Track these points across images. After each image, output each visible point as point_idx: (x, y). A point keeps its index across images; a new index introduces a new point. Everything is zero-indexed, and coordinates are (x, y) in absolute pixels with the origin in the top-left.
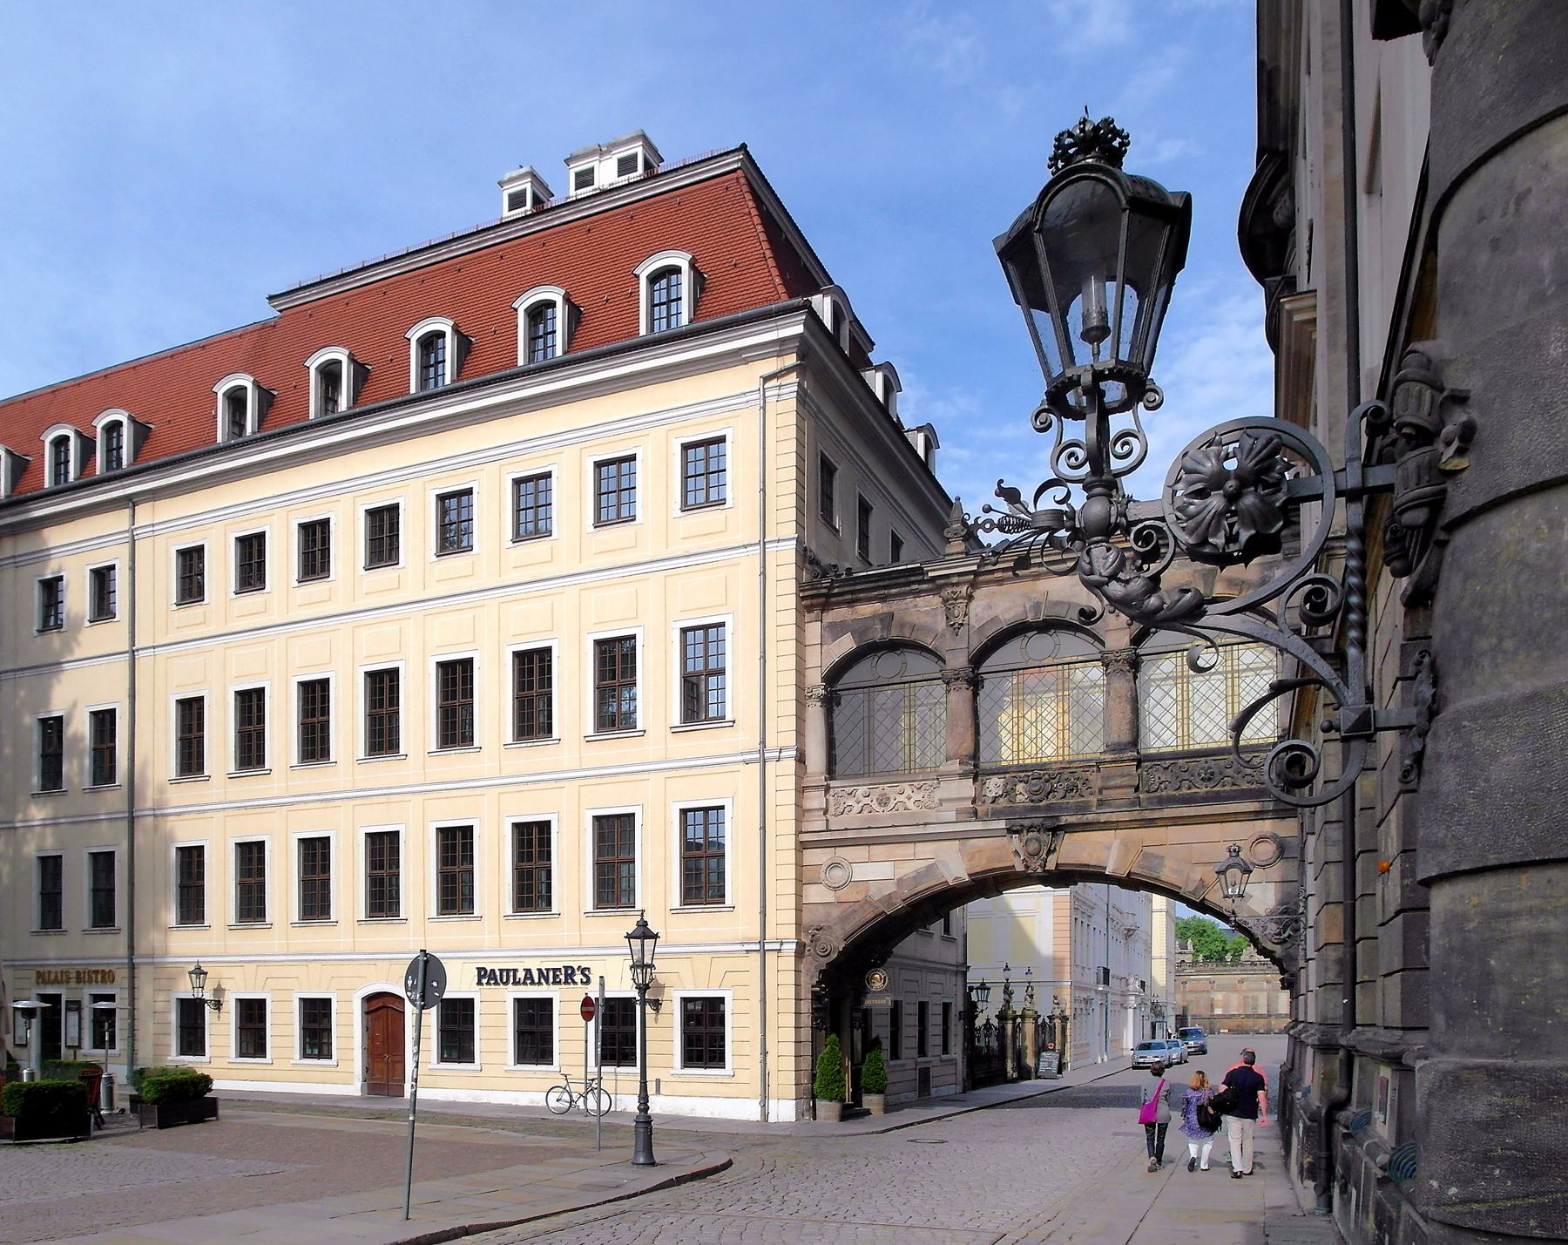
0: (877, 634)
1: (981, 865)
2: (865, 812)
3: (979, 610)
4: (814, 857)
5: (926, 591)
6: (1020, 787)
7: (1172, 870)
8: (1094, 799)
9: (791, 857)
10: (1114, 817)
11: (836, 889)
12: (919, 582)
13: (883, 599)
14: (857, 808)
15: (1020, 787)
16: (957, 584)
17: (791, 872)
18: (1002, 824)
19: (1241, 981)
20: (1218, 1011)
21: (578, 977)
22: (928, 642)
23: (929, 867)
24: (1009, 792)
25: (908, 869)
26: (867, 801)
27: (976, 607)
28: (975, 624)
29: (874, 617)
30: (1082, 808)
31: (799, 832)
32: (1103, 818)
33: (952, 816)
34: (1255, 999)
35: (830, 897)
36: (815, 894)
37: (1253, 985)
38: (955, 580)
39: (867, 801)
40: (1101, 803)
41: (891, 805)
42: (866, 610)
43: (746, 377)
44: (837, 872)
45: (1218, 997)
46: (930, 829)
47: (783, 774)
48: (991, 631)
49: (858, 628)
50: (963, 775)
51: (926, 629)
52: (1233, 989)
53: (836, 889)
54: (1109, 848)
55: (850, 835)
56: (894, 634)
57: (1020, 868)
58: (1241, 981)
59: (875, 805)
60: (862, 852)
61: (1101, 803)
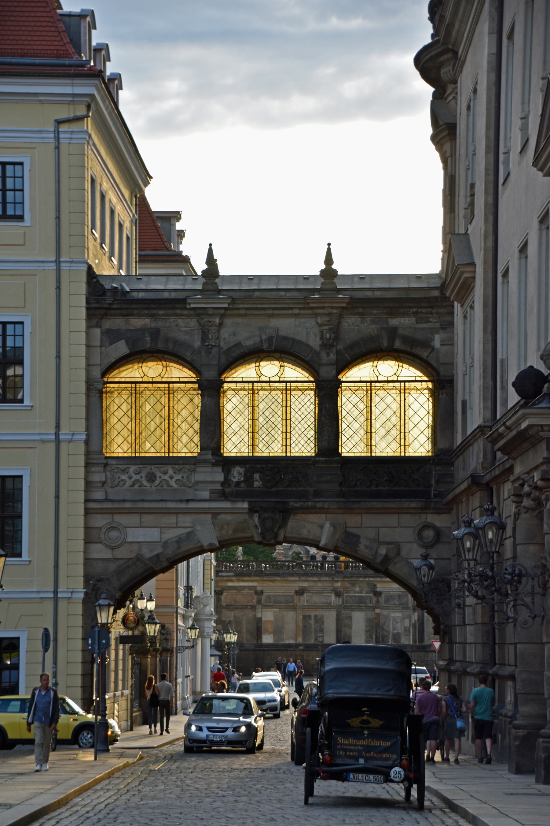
2: (136, 487)
3: (226, 335)
4: (100, 521)
5: (188, 316)
6: (257, 476)
7: (366, 547)
9: (81, 521)
10: (326, 505)
11: (113, 548)
12: (182, 309)
13: (151, 316)
14: (129, 483)
16: (211, 315)
17: (81, 533)
18: (246, 505)
19: (300, 592)
20: (267, 639)
22: (188, 355)
23: (189, 534)
24: (248, 479)
25: (172, 534)
26: (138, 477)
27: (225, 333)
28: (224, 346)
29: (143, 330)
31: (87, 501)
33: (206, 495)
34: (320, 620)
35: (107, 554)
36: (99, 552)
37: (317, 599)
38: (210, 312)
39: (138, 477)
41: (157, 482)
42: (138, 322)
43: (45, 118)
44: (114, 534)
45: (268, 616)
48: (238, 352)
49: (132, 338)
50: (214, 465)
52: (288, 604)
54: (322, 527)
55: (128, 505)
56: (160, 346)
58: (300, 592)
59: (144, 482)
60: (134, 519)
61: (317, 494)
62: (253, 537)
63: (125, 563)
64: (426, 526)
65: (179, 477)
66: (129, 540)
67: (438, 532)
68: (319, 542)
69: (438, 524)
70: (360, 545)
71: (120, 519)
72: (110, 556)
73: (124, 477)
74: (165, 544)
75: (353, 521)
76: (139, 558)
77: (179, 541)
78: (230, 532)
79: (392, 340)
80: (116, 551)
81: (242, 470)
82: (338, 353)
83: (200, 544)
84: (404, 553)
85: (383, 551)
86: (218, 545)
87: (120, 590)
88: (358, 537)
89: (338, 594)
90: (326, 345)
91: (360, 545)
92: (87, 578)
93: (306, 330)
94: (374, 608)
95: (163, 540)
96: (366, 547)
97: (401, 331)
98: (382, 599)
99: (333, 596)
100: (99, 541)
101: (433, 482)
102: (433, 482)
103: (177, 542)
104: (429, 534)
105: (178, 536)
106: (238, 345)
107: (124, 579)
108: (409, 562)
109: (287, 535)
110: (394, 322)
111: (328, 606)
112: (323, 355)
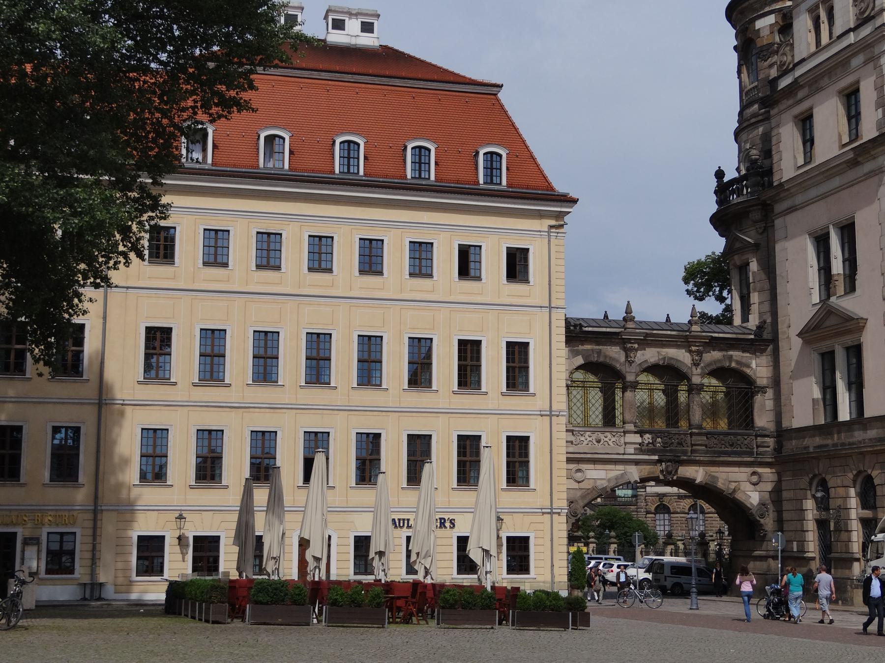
0: (594, 358)
1: (645, 474)
8: (690, 449)
14: (586, 442)
15: (659, 440)
21: (448, 524)
23: (622, 474)
26: (590, 439)
30: (685, 453)
32: (697, 458)
33: (632, 451)
39: (590, 439)
40: (693, 451)
44: (579, 474)
46: (626, 457)
47: (560, 423)
48: (645, 366)
50: (636, 433)
51: (617, 361)
53: (579, 482)
54: (697, 471)
57: (662, 477)
60: (591, 466)
61: (693, 451)
65: (614, 439)
71: (583, 466)
73: (583, 438)
74: (609, 480)
76: (594, 488)
77: (617, 478)
79: (730, 362)
81: (650, 436)
82: (702, 368)
84: (742, 488)
85: (733, 486)
90: (696, 364)
93: (681, 356)
97: (734, 358)
106: (646, 361)
110: (731, 353)
112: (694, 368)
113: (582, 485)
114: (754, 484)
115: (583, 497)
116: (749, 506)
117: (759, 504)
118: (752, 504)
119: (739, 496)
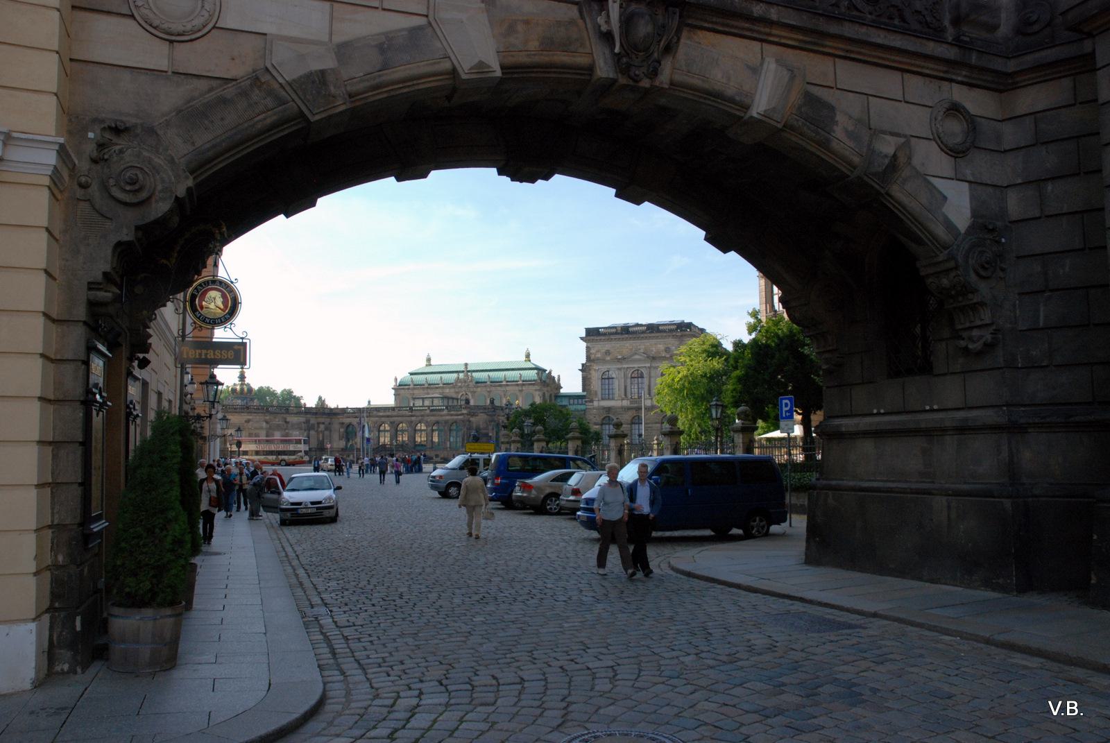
7: (846, 131)
11: (172, 39)
23: (414, 31)
35: (156, 56)
54: (755, 71)
58: (248, 421)
62: (591, 69)
63: (211, 89)
64: (955, 109)
66: (229, 21)
67: (972, 123)
68: (747, 108)
69: (972, 108)
70: (835, 128)
72: (163, 64)
74: (343, 50)
75: (818, 68)
76: (258, 80)
77: (386, 45)
78: (534, 45)
80: (182, 51)
83: (446, 65)
84: (916, 161)
85: (887, 146)
86: (498, 73)
87: (192, 173)
88: (832, 109)
89: (267, 422)
91: (835, 128)
92: (73, 121)
94: (285, 429)
95: (337, 39)
96: (850, 135)
98: (289, 426)
99: (265, 424)
100: (125, 11)
101: (947, 23)
102: (947, 23)
103: (381, 48)
104: (955, 129)
105: (386, 34)
107: (204, 139)
108: (929, 182)
109: (678, 78)
111: (262, 428)
113: (196, 58)
114: (956, 153)
115: (192, 115)
116: (940, 231)
117: (972, 229)
118: (949, 226)
119: (903, 193)
